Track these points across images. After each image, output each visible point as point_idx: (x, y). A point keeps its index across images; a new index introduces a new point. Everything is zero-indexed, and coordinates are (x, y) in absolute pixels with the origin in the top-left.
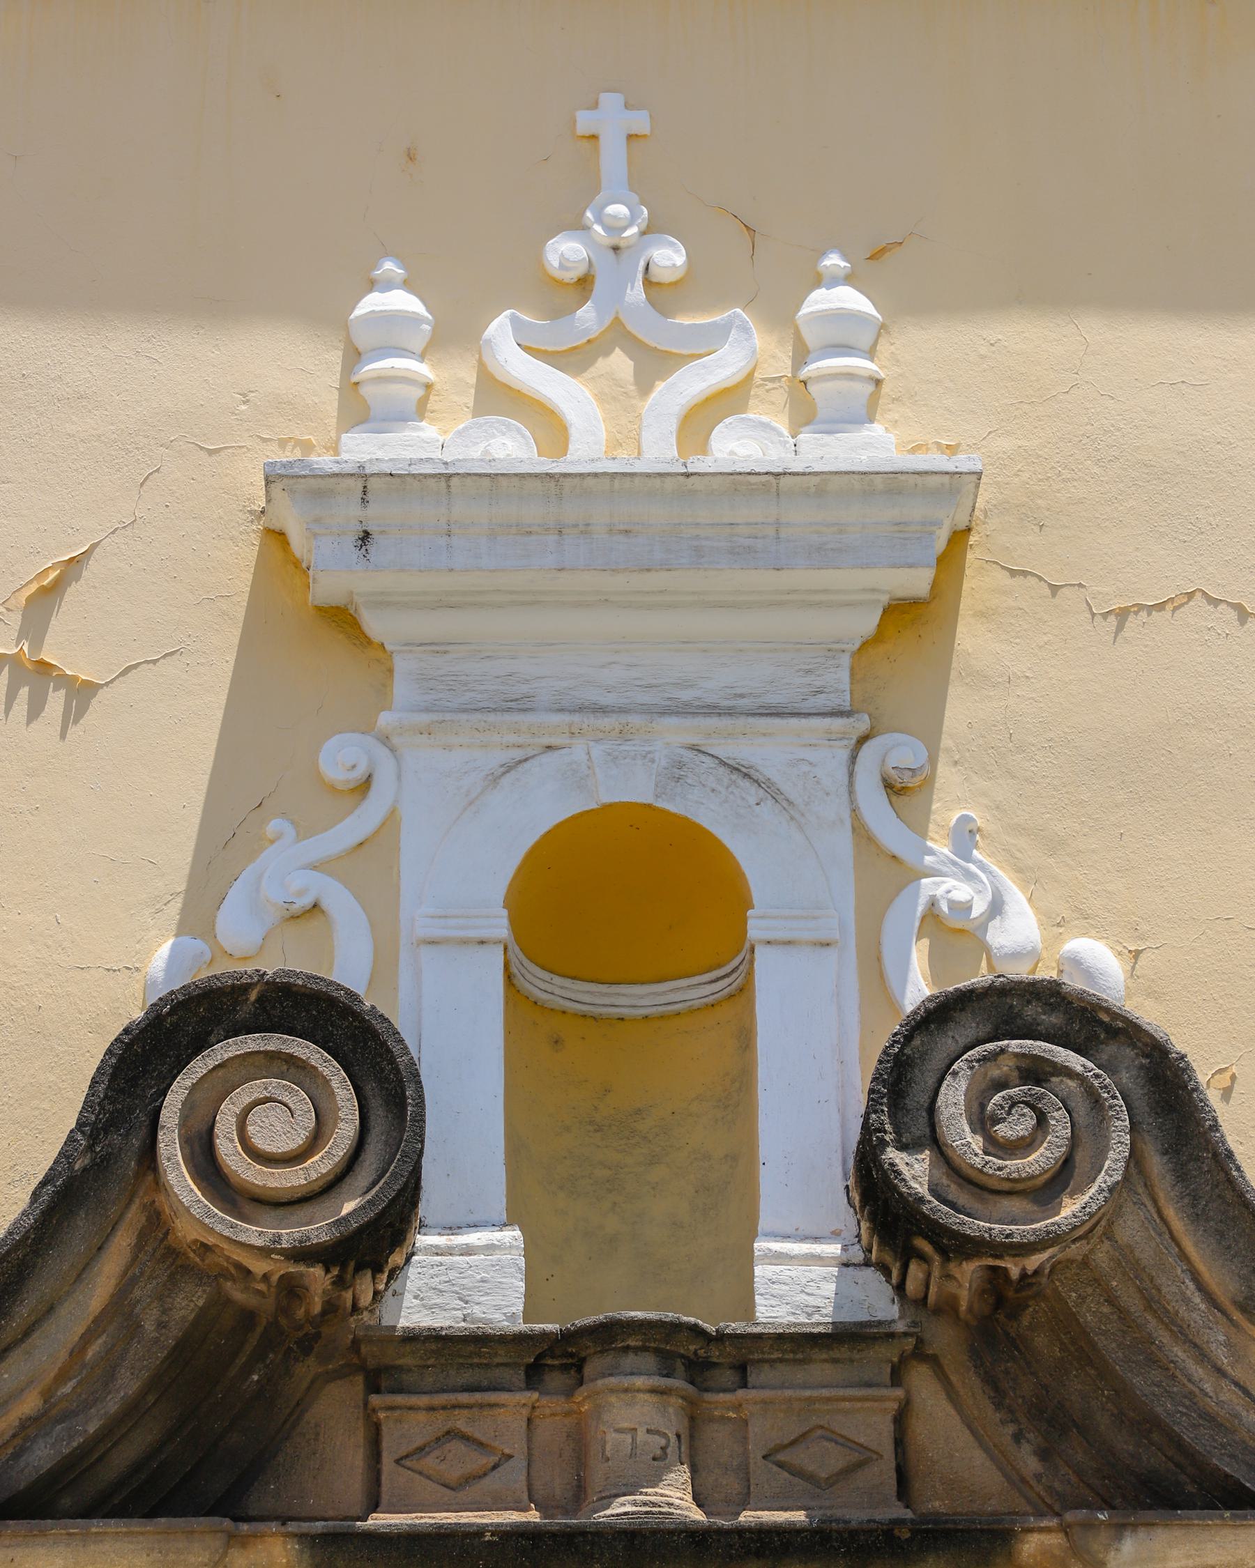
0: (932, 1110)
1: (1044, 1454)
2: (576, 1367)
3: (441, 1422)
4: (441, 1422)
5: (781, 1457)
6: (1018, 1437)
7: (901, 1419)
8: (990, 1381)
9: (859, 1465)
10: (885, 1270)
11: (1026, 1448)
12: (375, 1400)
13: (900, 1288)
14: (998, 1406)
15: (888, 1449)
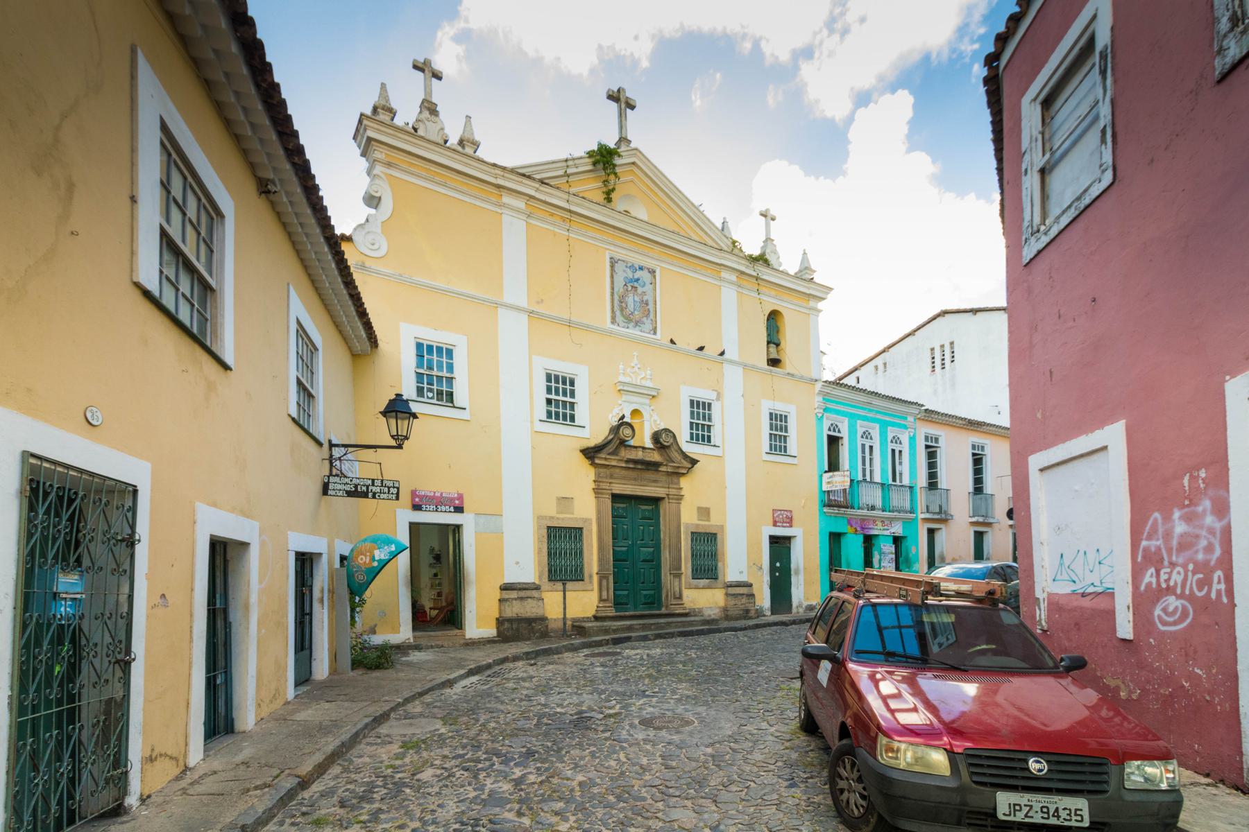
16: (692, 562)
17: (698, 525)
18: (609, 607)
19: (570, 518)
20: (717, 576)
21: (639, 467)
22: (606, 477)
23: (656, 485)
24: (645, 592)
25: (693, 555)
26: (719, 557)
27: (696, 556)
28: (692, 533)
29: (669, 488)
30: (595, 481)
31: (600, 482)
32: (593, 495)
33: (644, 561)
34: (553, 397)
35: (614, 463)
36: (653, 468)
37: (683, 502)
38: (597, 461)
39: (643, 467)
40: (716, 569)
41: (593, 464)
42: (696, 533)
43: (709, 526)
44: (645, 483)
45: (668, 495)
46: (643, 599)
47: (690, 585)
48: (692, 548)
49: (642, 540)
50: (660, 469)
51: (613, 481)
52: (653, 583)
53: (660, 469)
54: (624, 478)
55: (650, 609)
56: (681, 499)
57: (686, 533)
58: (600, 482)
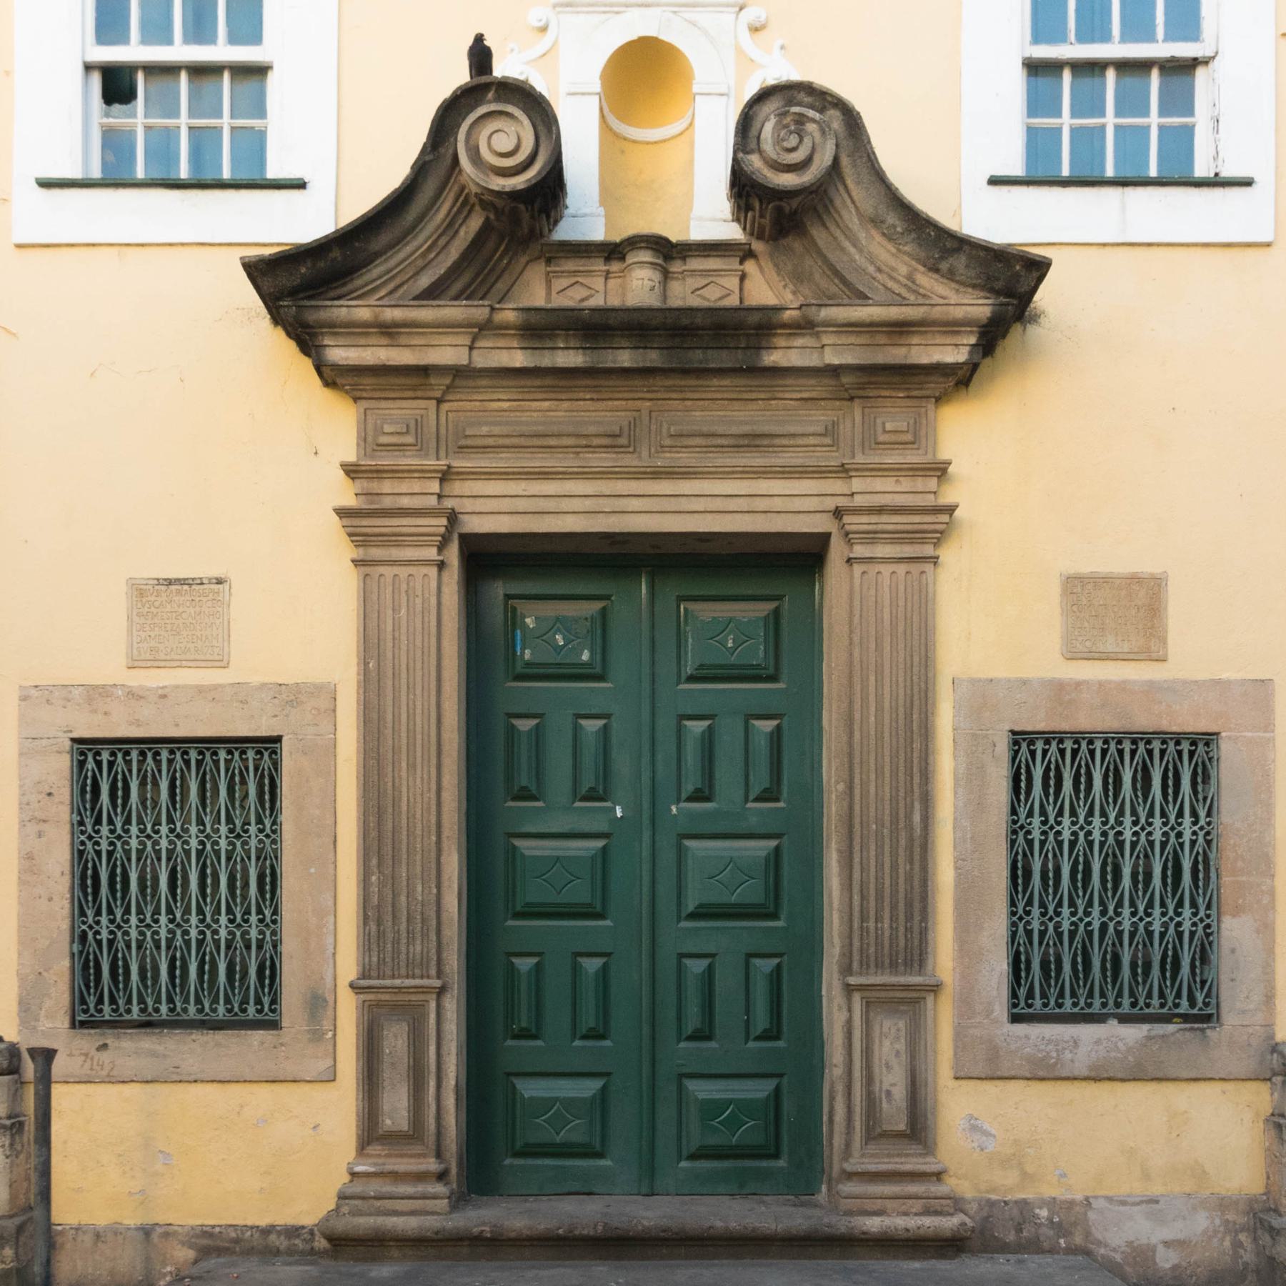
0: (758, 138)
1: (794, 293)
2: (623, 258)
3: (573, 280)
4: (573, 280)
5: (698, 293)
6: (785, 286)
7: (743, 277)
8: (776, 265)
9: (729, 295)
10: (738, 220)
11: (788, 290)
12: (548, 269)
13: (744, 229)
14: (778, 275)
15: (737, 291)
16: (1017, 918)
17: (1060, 691)
18: (420, 1177)
19: (201, 690)
20: (1211, 992)
21: (625, 358)
22: (419, 447)
23: (757, 460)
24: (701, 1090)
25: (1018, 875)
26: (1228, 883)
27: (1051, 878)
28: (1019, 739)
29: (844, 471)
30: (352, 471)
31: (378, 473)
32: (348, 551)
33: (704, 913)
34: (131, 52)
35: (448, 353)
36: (722, 359)
37: (949, 554)
38: (339, 354)
39: (653, 358)
40: (1204, 956)
41: (331, 376)
42: (1048, 737)
43: (1152, 689)
44: (684, 458)
45: (838, 513)
46: (695, 1137)
47: (994, 1054)
48: (1016, 828)
49: (699, 796)
50: (772, 358)
51: (459, 463)
52: (765, 1036)
53: (772, 358)
54: (539, 440)
55: (742, 1187)
56: (940, 536)
57: (971, 743)
58: (378, 473)
